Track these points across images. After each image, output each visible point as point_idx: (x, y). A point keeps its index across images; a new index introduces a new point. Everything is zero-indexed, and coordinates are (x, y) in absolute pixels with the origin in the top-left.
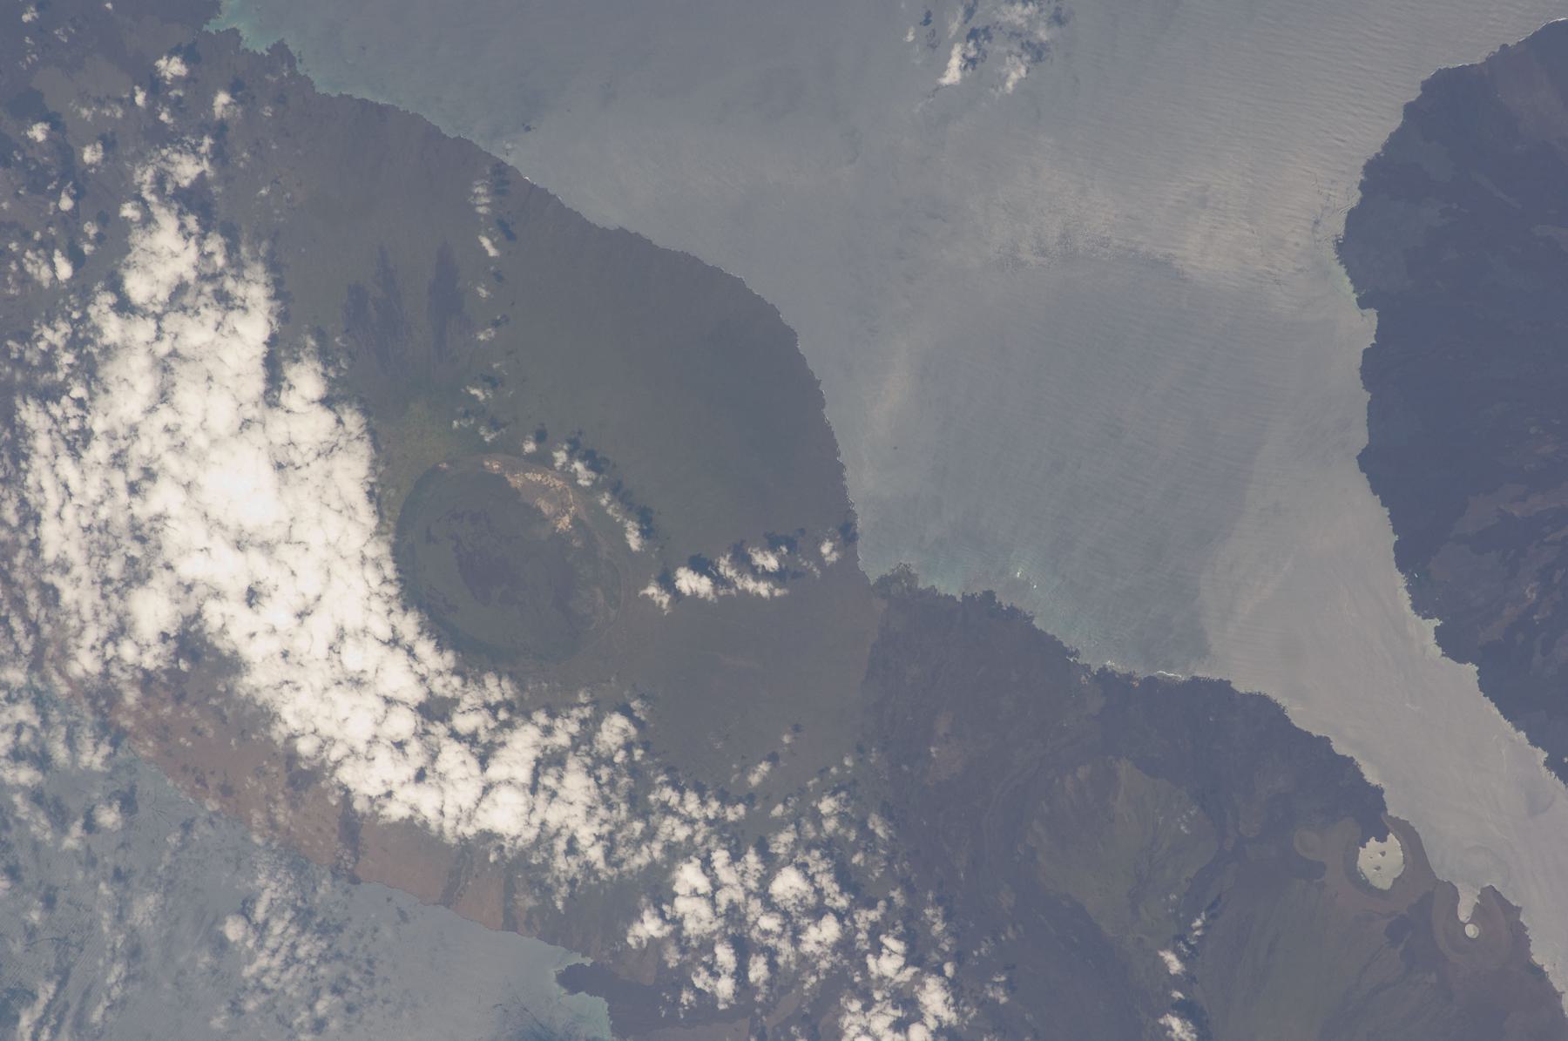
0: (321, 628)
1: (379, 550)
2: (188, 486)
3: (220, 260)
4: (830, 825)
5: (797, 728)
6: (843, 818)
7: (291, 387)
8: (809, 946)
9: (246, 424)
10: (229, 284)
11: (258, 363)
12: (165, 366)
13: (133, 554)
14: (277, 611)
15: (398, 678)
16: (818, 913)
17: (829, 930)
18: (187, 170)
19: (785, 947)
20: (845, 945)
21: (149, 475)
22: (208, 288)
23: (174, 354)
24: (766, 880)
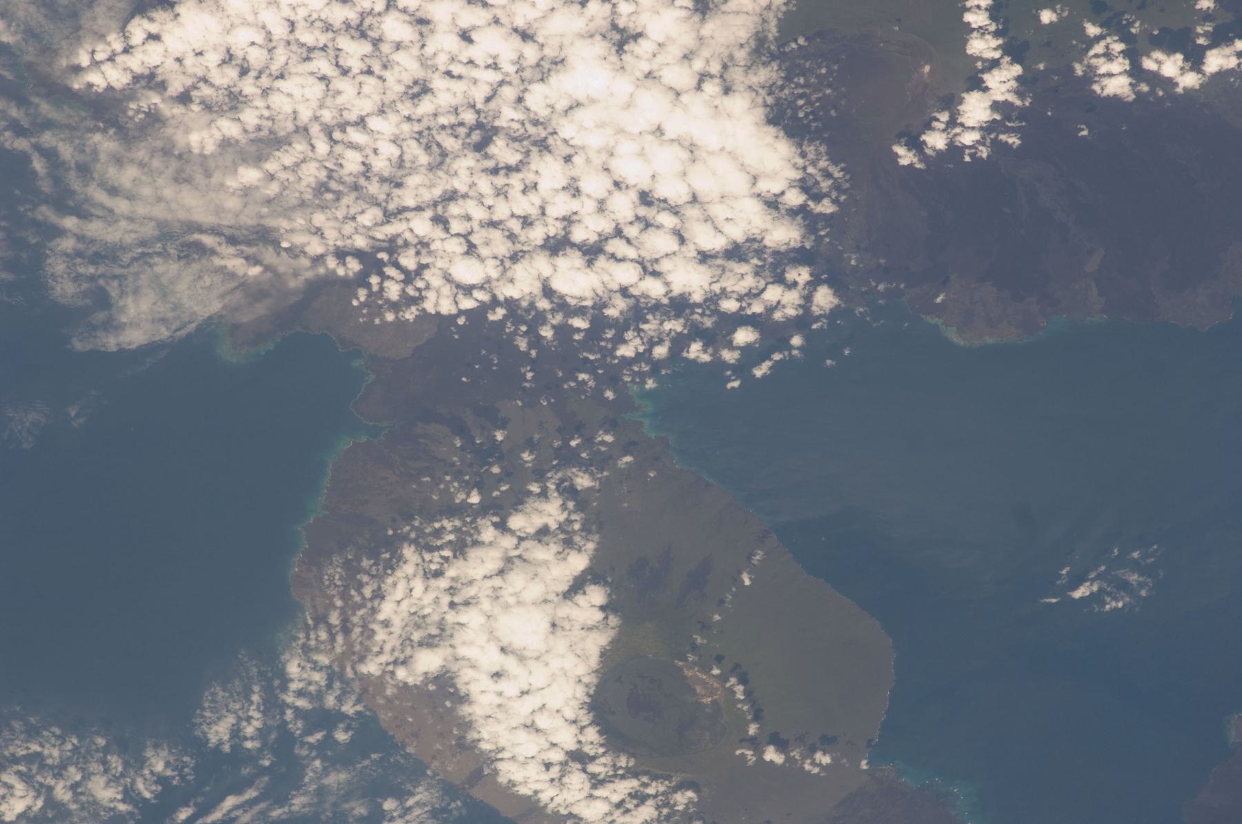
0: (531, 702)
1: (593, 679)
2: (489, 617)
3: (577, 526)
7: (584, 593)
9: (546, 601)
10: (577, 539)
11: (571, 578)
12: (509, 560)
13: (438, 636)
14: (510, 688)
15: (567, 738)
18: (583, 481)
21: (467, 603)
22: (562, 536)
23: (520, 557)
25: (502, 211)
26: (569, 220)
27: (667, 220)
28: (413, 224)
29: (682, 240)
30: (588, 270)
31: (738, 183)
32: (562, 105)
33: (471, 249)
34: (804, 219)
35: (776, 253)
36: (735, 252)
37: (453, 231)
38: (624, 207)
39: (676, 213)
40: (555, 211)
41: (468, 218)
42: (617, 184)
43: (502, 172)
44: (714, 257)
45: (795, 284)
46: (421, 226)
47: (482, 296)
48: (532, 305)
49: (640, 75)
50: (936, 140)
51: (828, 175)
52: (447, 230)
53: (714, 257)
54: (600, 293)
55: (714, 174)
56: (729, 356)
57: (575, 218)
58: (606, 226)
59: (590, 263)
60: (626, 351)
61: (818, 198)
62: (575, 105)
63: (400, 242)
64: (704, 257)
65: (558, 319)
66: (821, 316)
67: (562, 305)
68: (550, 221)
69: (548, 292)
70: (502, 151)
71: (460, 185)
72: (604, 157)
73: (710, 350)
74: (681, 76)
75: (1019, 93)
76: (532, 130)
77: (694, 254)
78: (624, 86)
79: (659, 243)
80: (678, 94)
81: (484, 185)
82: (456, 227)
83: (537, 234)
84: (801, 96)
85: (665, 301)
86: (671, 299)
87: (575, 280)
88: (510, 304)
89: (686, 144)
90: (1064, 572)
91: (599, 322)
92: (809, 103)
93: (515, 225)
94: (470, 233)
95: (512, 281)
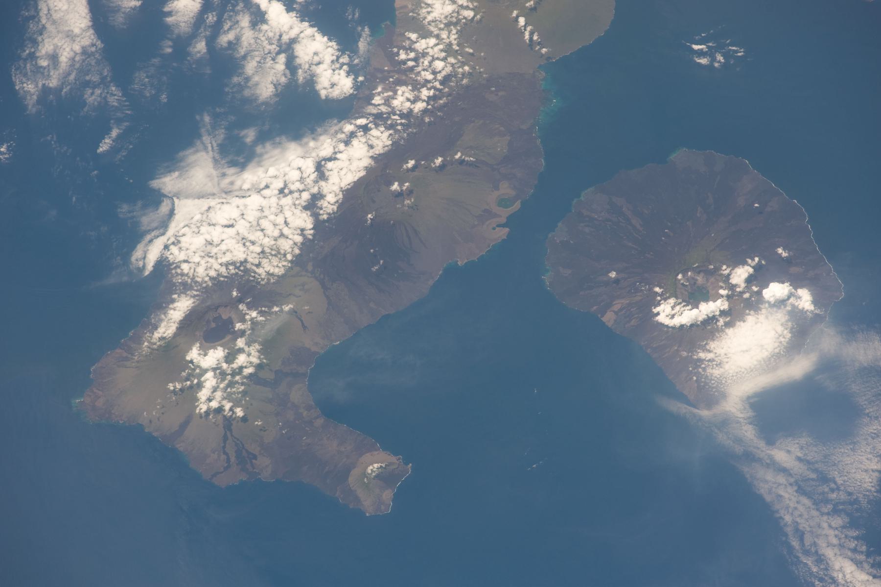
4: (460, 70)
5: (485, 59)
6: (463, 74)
8: (423, 73)
16: (434, 73)
17: (430, 77)
19: (420, 69)
20: (427, 81)
24: (438, 59)
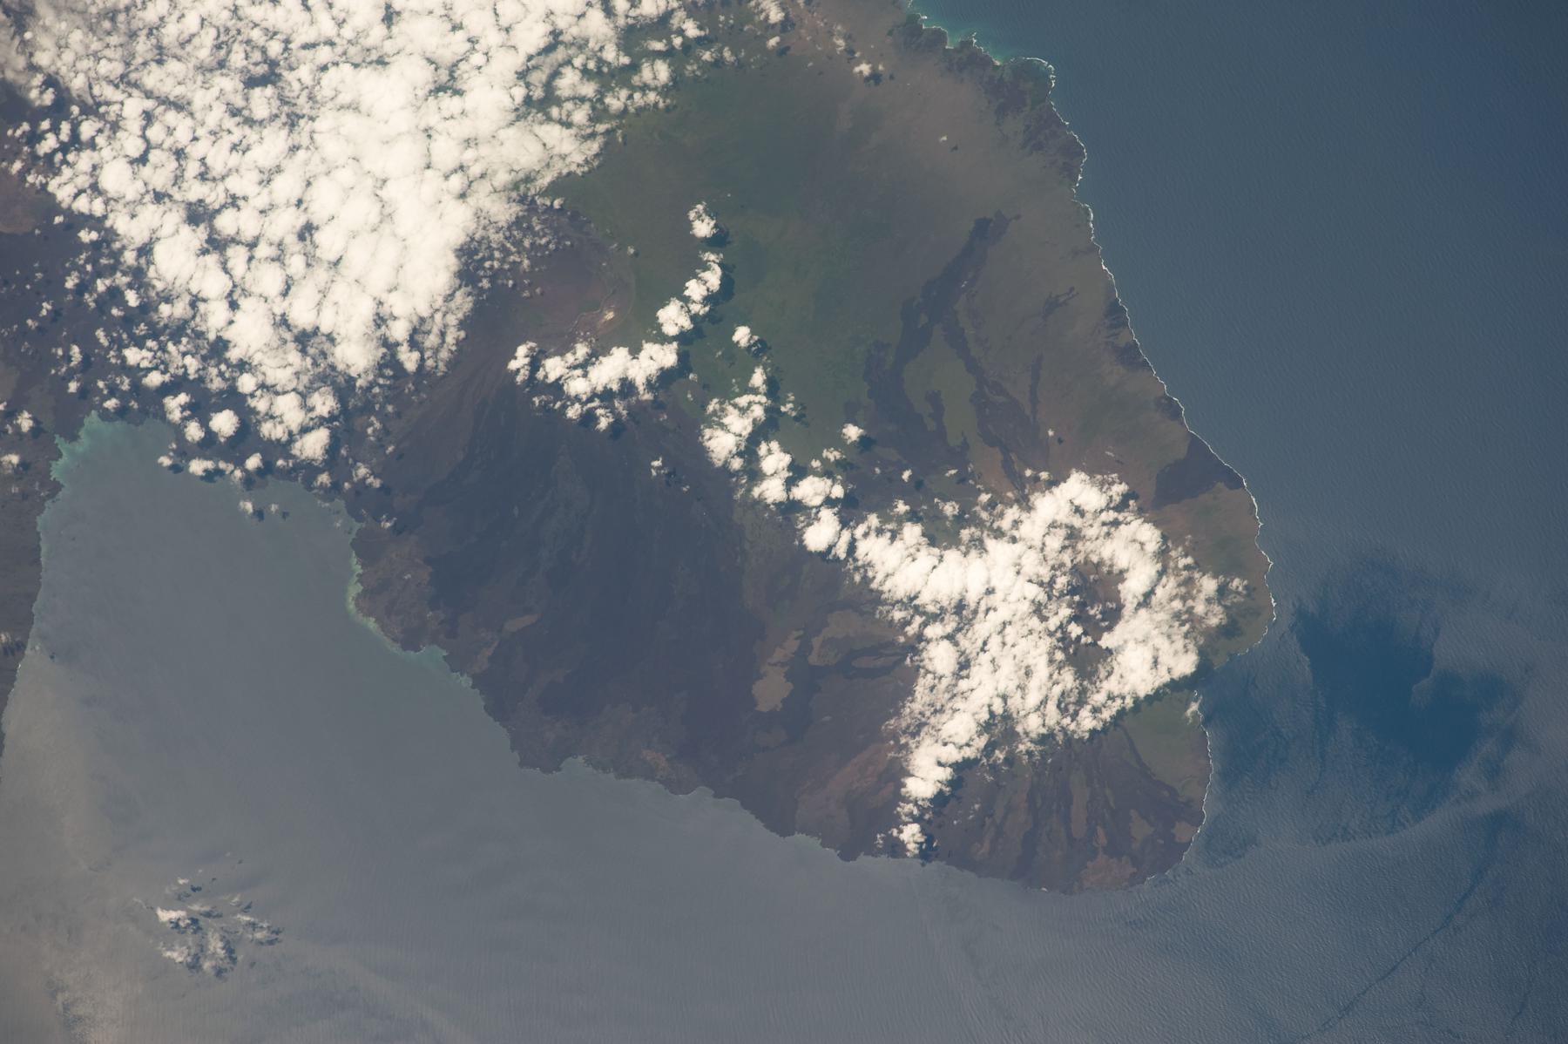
25: (196, 151)
26: (234, 201)
27: (296, 264)
28: (129, 103)
29: (285, 294)
30: (193, 258)
31: (378, 281)
32: (345, 98)
33: (143, 160)
34: (384, 355)
35: (333, 367)
36: (304, 339)
37: (149, 133)
38: (285, 224)
39: (308, 265)
40: (235, 185)
41: (170, 131)
42: (300, 202)
43: (237, 119)
44: (289, 327)
45: (312, 409)
46: (133, 107)
47: (98, 208)
48: (124, 248)
49: (423, 126)
50: (554, 368)
51: (443, 334)
52: (144, 129)
53: (289, 327)
54: (178, 283)
55: (373, 255)
56: (194, 432)
57: (241, 203)
58: (248, 234)
59: (204, 252)
60: (133, 355)
61: (414, 344)
62: (354, 107)
63: (102, 109)
64: (283, 322)
65: (122, 280)
66: (294, 457)
67: (138, 277)
68: (221, 187)
69: (145, 251)
70: (261, 102)
71: (200, 99)
72: (322, 168)
73: (187, 413)
74: (446, 151)
75: (649, 385)
76: (302, 100)
77: (278, 311)
78: (403, 121)
79: (269, 279)
80: (428, 167)
81: (216, 116)
82: (155, 133)
83: (195, 191)
84: (503, 249)
85: (212, 336)
86: (219, 338)
87: (177, 260)
88: (109, 236)
89: (387, 210)
90: (181, 882)
91: (147, 308)
92: (503, 261)
93: (193, 168)
94: (159, 146)
95: (133, 216)
